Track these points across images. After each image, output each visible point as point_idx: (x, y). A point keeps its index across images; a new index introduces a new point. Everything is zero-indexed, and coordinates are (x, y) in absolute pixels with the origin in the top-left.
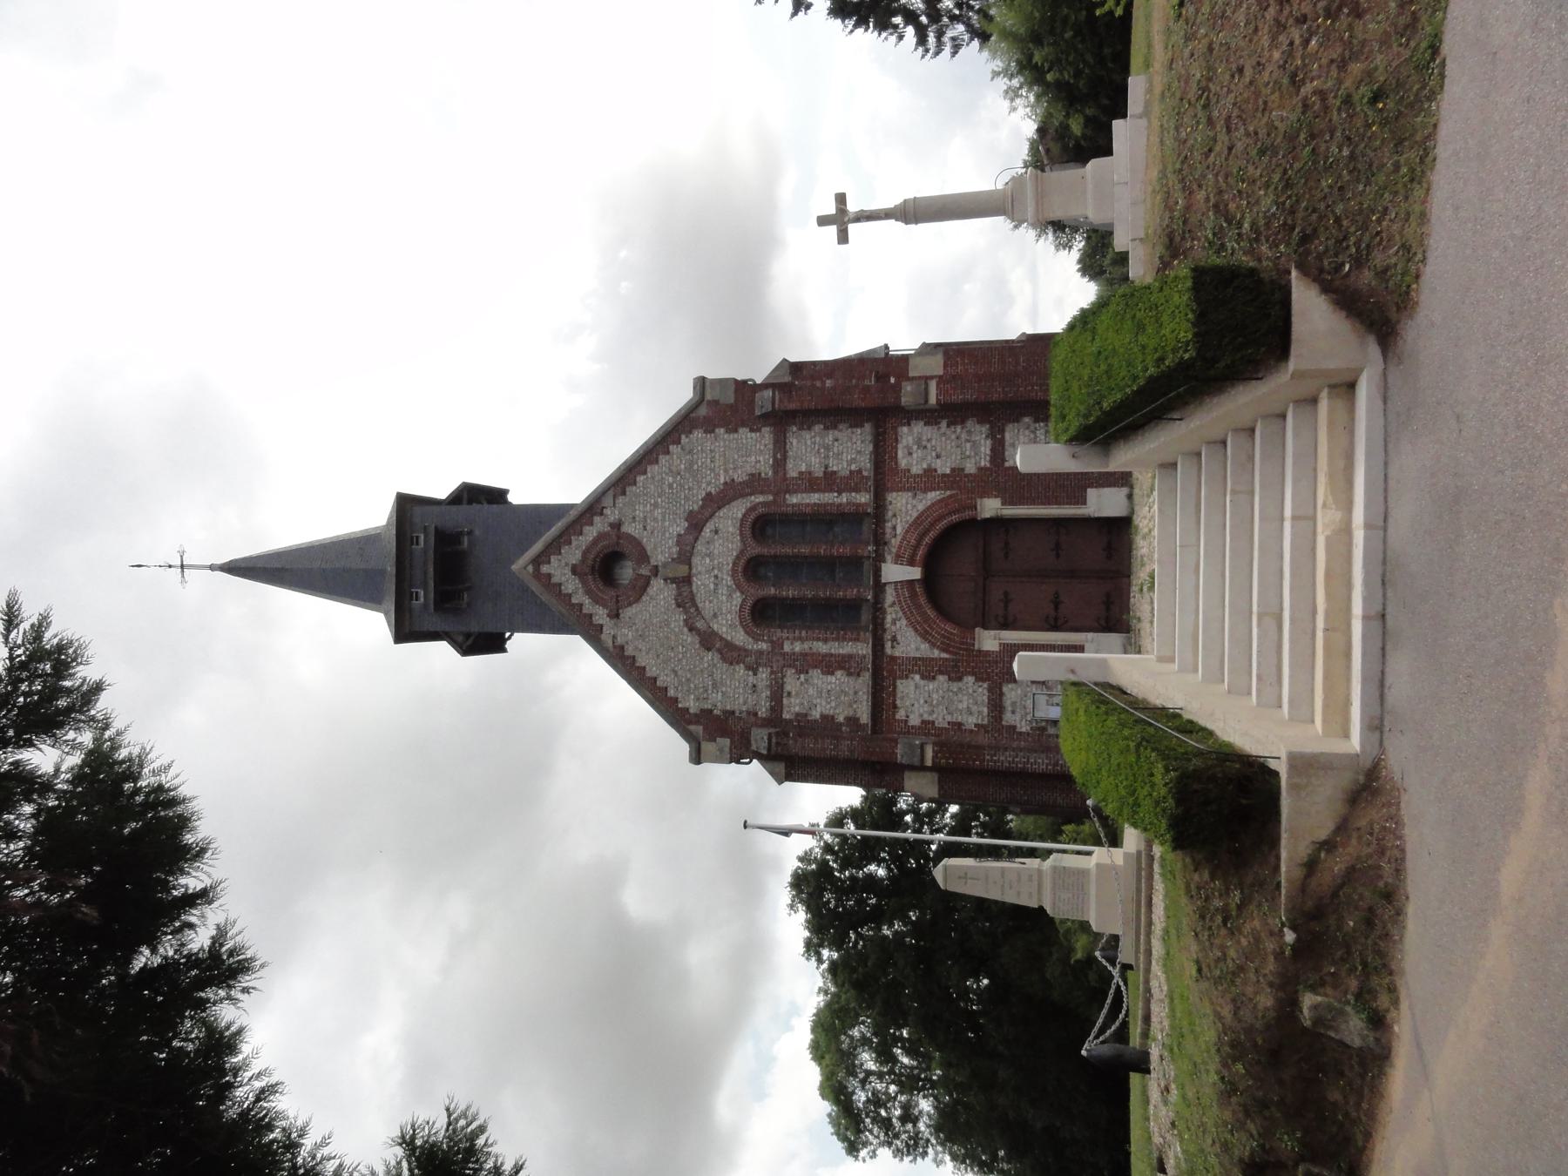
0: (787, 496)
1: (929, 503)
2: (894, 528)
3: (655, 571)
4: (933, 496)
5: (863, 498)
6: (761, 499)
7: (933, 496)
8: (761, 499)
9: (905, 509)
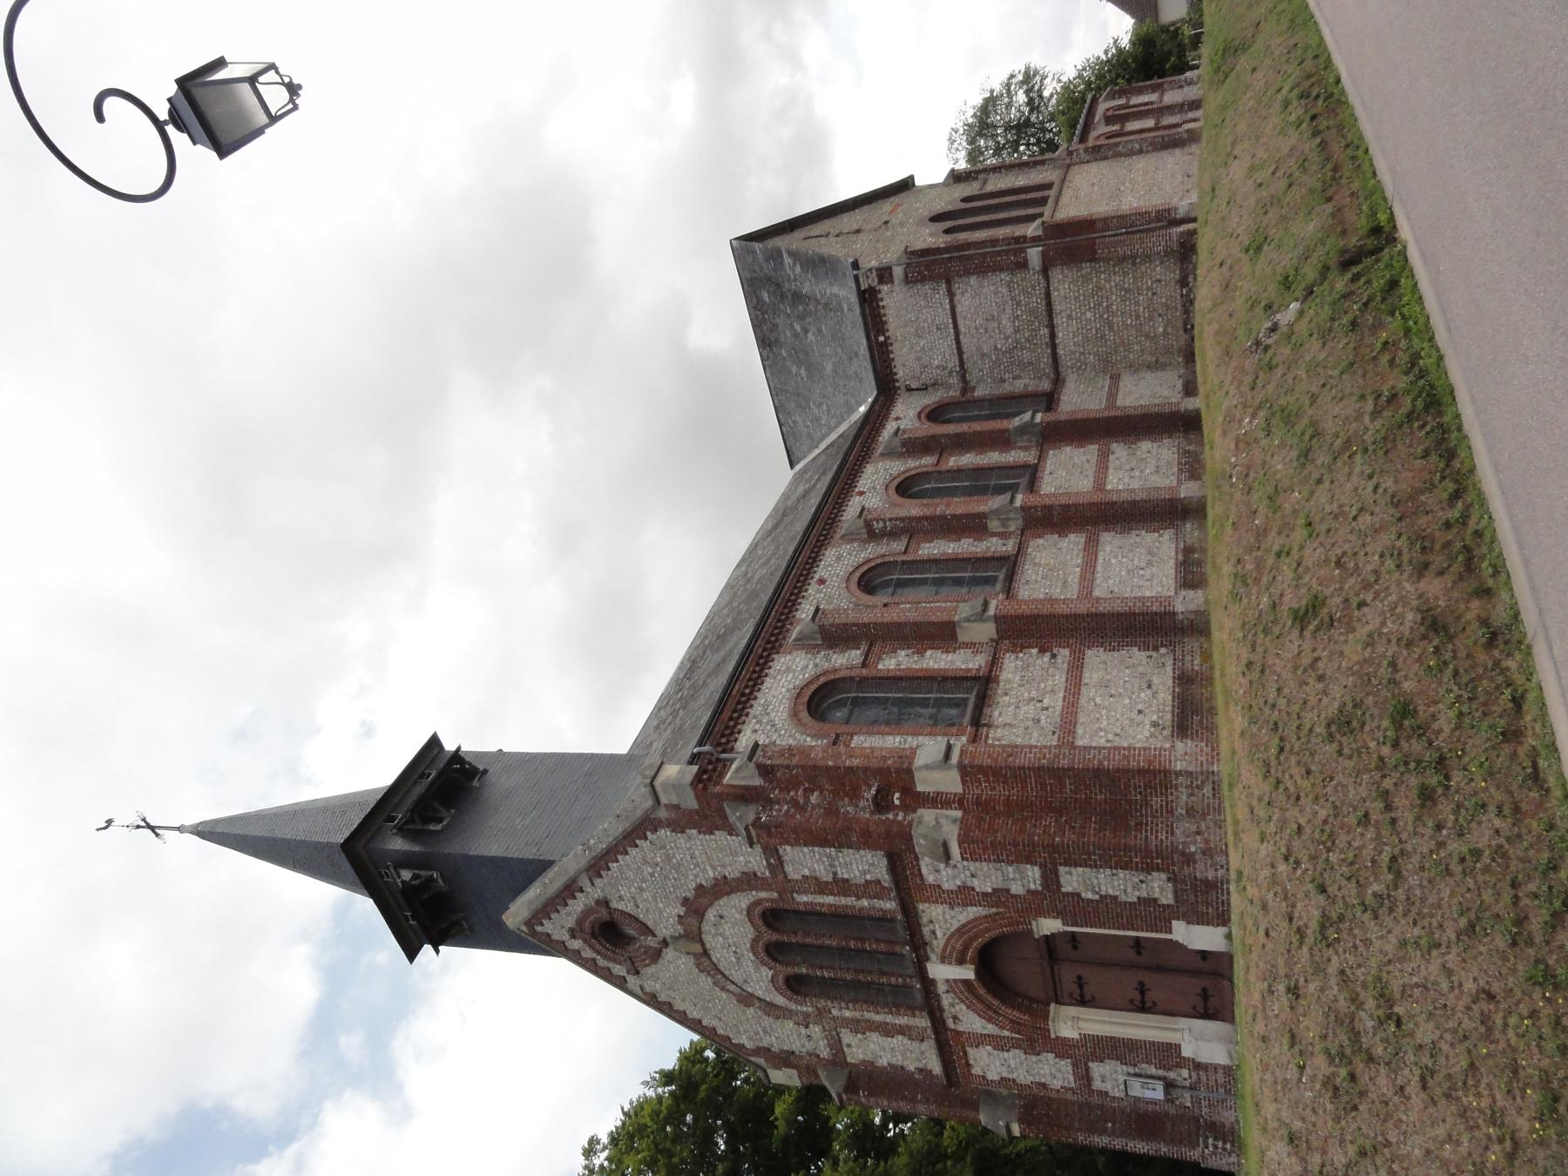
0: (795, 895)
1: (972, 917)
2: (934, 932)
3: (665, 943)
4: (973, 912)
5: (890, 905)
6: (763, 895)
7: (973, 912)
8: (763, 895)
9: (940, 921)
